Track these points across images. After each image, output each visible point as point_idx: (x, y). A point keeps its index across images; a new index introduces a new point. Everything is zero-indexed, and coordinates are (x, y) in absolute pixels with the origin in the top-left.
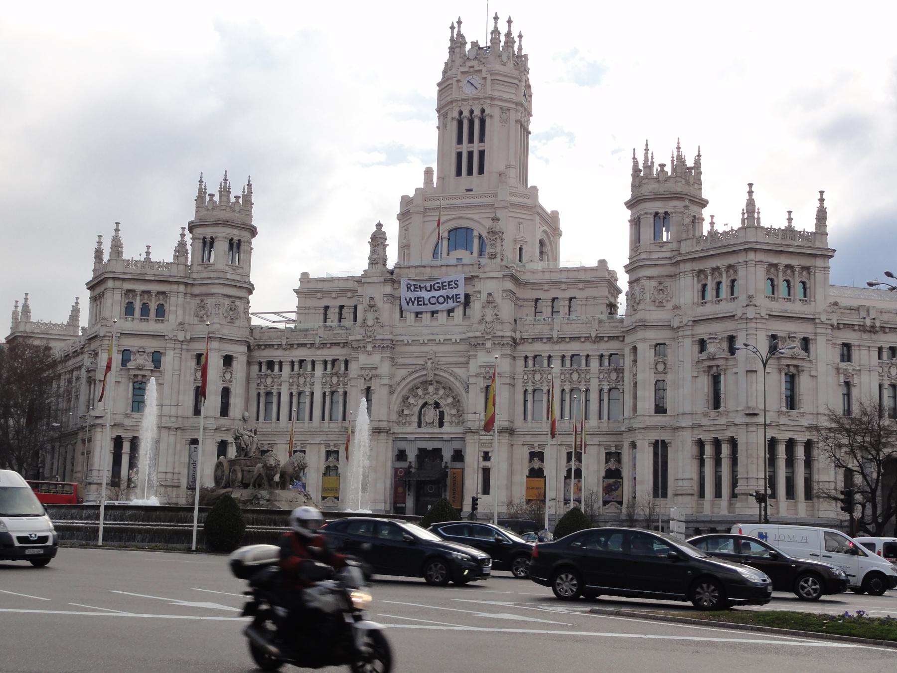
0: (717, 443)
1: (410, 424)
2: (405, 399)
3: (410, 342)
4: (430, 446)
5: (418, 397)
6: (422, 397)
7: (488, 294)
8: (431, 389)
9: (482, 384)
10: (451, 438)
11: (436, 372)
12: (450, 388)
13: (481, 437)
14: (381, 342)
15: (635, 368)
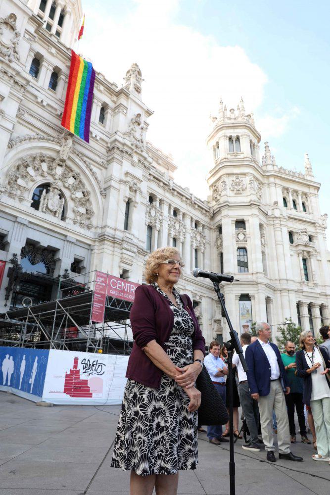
0: (310, 307)
1: (21, 200)
2: (22, 166)
3: (45, 104)
4: (45, 241)
5: (40, 172)
6: (46, 174)
7: (139, 115)
8: (59, 171)
9: (126, 192)
10: (77, 240)
11: (72, 156)
12: (80, 181)
13: (124, 251)
14: (14, 73)
15: (241, 237)
